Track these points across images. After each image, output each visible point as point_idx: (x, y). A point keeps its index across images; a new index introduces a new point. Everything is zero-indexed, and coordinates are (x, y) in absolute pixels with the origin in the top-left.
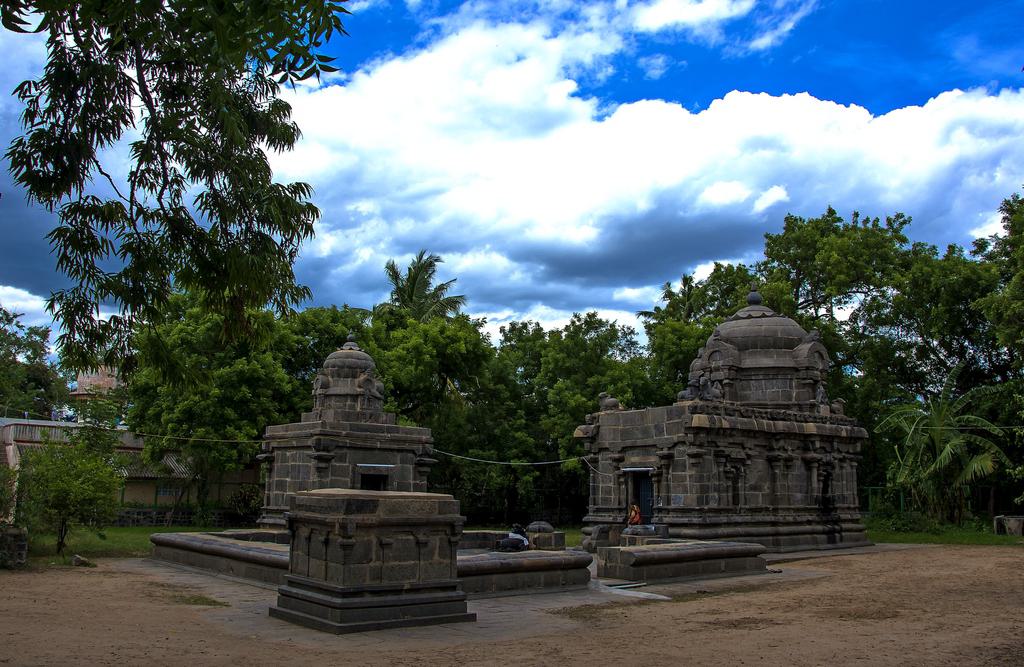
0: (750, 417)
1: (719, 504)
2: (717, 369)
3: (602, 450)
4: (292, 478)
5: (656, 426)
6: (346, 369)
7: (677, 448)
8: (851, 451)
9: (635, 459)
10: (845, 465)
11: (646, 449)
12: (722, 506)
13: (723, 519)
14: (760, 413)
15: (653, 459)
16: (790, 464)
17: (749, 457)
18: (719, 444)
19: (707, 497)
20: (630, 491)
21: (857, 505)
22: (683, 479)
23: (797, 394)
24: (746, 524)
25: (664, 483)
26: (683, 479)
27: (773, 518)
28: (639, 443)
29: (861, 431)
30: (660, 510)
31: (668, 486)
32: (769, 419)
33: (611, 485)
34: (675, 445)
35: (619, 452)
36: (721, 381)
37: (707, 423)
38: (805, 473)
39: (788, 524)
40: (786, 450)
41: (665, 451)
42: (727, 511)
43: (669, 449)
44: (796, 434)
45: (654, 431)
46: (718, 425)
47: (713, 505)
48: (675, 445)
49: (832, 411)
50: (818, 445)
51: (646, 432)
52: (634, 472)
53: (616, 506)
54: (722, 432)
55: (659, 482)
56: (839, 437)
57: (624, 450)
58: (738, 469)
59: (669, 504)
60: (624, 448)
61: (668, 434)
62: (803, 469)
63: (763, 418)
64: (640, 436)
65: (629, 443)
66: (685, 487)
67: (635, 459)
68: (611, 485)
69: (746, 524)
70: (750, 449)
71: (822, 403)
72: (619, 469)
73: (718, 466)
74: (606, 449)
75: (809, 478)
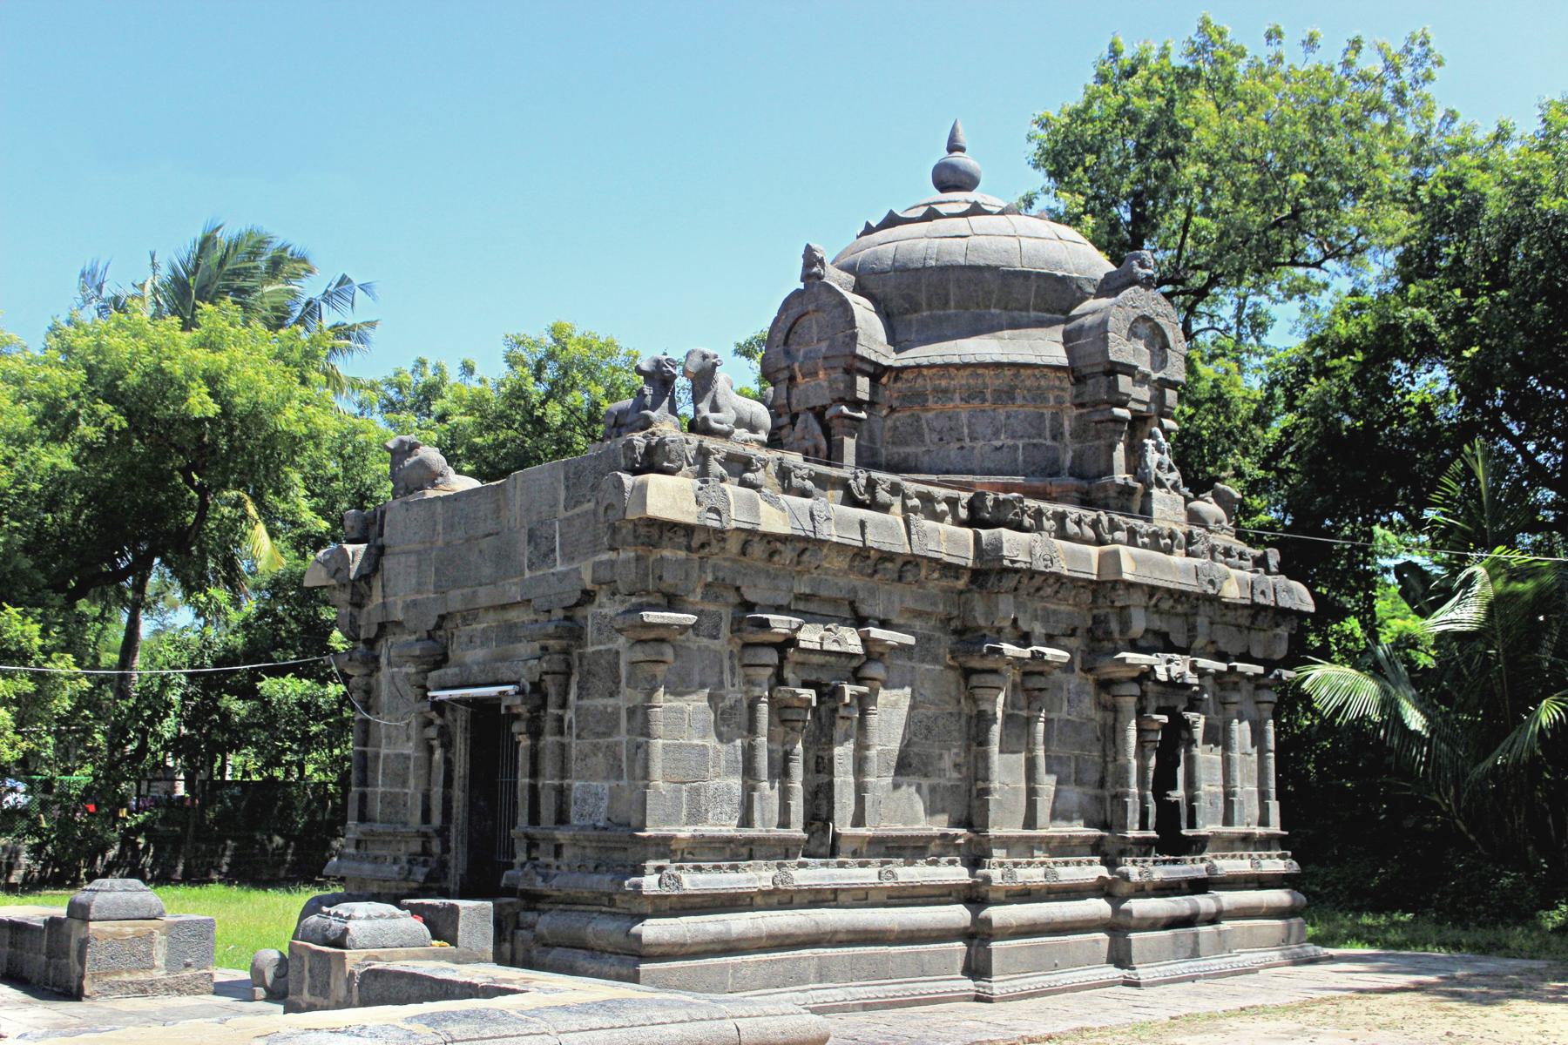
0: (885, 508)
1: (746, 822)
7: (591, 610)
8: (1257, 652)
10: (1235, 697)
12: (755, 832)
13: (757, 876)
14: (927, 499)
16: (1035, 682)
17: (873, 651)
18: (750, 596)
19: (695, 793)
20: (461, 768)
21: (1275, 827)
22: (609, 723)
23: (1078, 456)
24: (863, 898)
25: (549, 740)
26: (609, 723)
27: (957, 874)
28: (485, 596)
29: (1289, 591)
32: (962, 524)
34: (588, 597)
36: (819, 413)
37: (694, 507)
38: (1098, 716)
39: (1026, 895)
40: (1024, 639)
42: (782, 851)
44: (1058, 577)
45: (524, 552)
46: (737, 517)
47: (726, 826)
49: (1194, 517)
50: (1139, 624)
52: (460, 701)
54: (758, 550)
55: (536, 733)
56: (1214, 600)
58: (828, 693)
60: (442, 618)
61: (568, 557)
62: (1088, 706)
63: (939, 517)
64: (487, 571)
65: (455, 600)
66: (612, 751)
68: (409, 749)
69: (863, 898)
70: (884, 624)
71: (1160, 484)
72: (425, 697)
73: (750, 682)
74: (399, 624)
75: (1111, 737)
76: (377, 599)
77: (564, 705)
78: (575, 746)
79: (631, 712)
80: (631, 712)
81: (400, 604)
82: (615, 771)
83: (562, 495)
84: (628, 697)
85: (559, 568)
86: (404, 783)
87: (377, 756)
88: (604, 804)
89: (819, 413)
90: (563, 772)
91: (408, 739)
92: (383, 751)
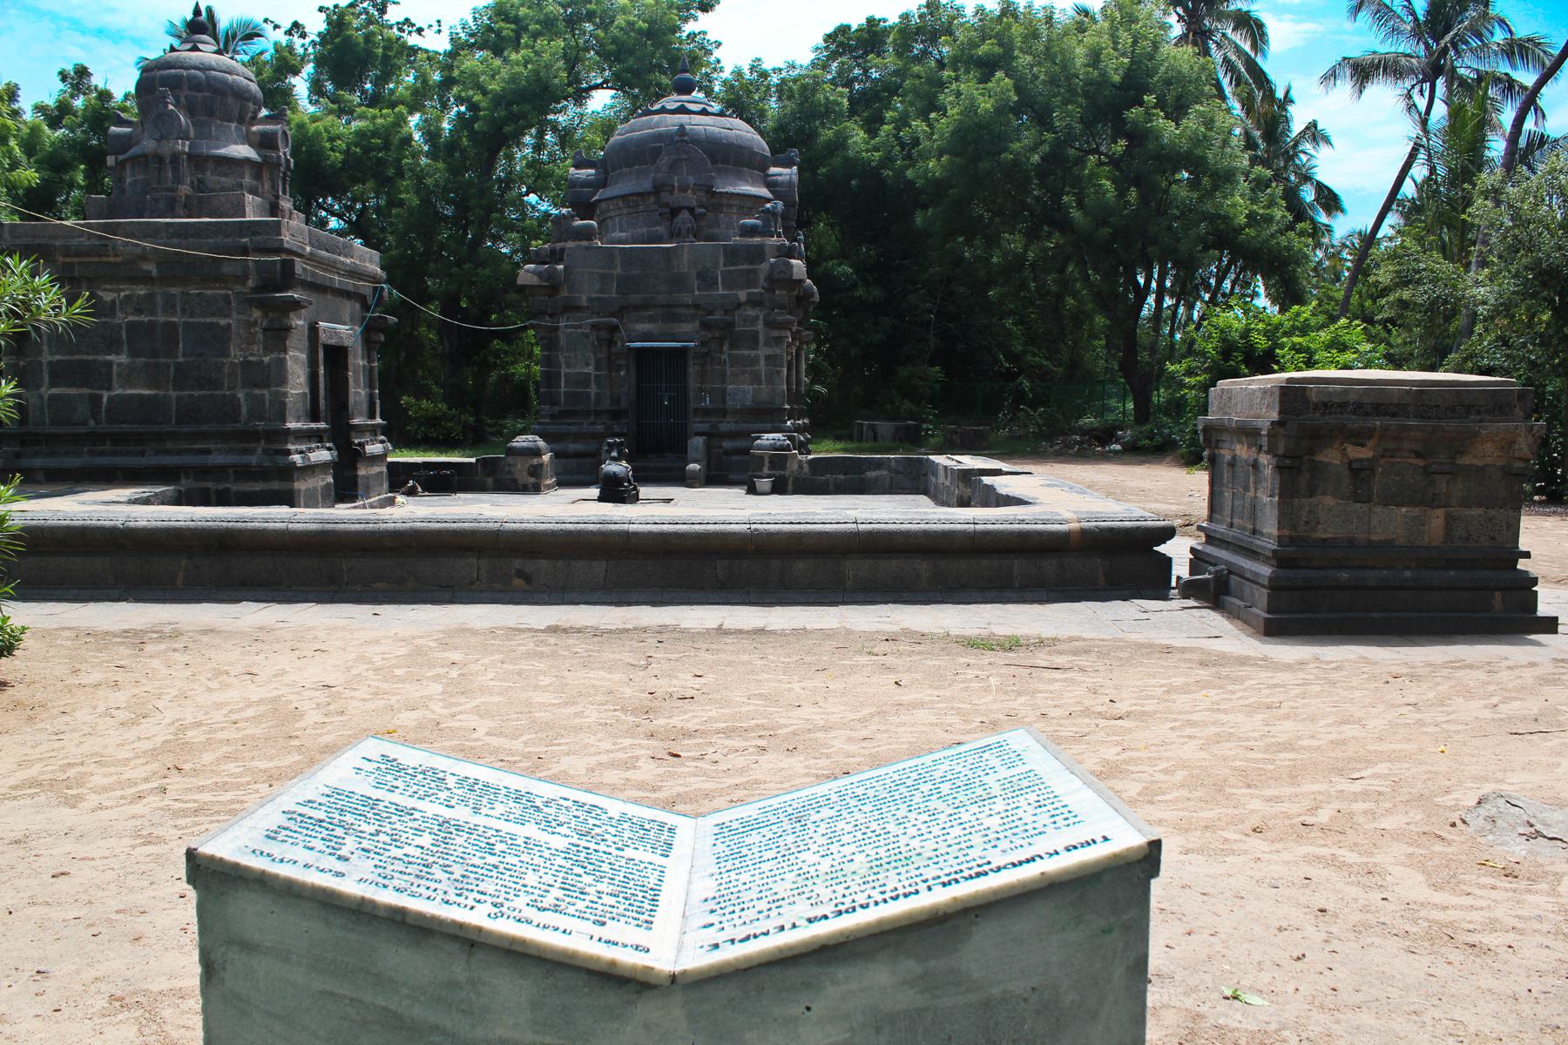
2: (684, 189)
3: (572, 308)
4: (134, 353)
5: (699, 275)
6: (230, 100)
9: (642, 327)
11: (670, 313)
15: (687, 327)
22: (755, 361)
28: (661, 299)
30: (706, 412)
31: (723, 373)
33: (590, 369)
34: (739, 305)
35: (612, 315)
36: (691, 210)
41: (718, 316)
43: (726, 312)
48: (739, 305)
51: (678, 283)
53: (606, 404)
57: (621, 311)
59: (724, 401)
61: (725, 286)
65: (635, 298)
67: (642, 327)
68: (590, 369)
74: (579, 308)
76: (564, 293)
77: (722, 352)
78: (728, 371)
79: (767, 358)
80: (767, 358)
81: (584, 298)
82: (756, 379)
83: (722, 260)
84: (763, 352)
85: (721, 292)
86: (587, 385)
87: (559, 374)
88: (749, 396)
89: (691, 210)
90: (723, 381)
91: (587, 364)
92: (563, 371)
